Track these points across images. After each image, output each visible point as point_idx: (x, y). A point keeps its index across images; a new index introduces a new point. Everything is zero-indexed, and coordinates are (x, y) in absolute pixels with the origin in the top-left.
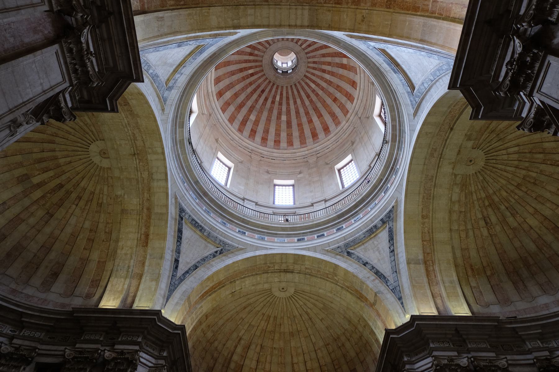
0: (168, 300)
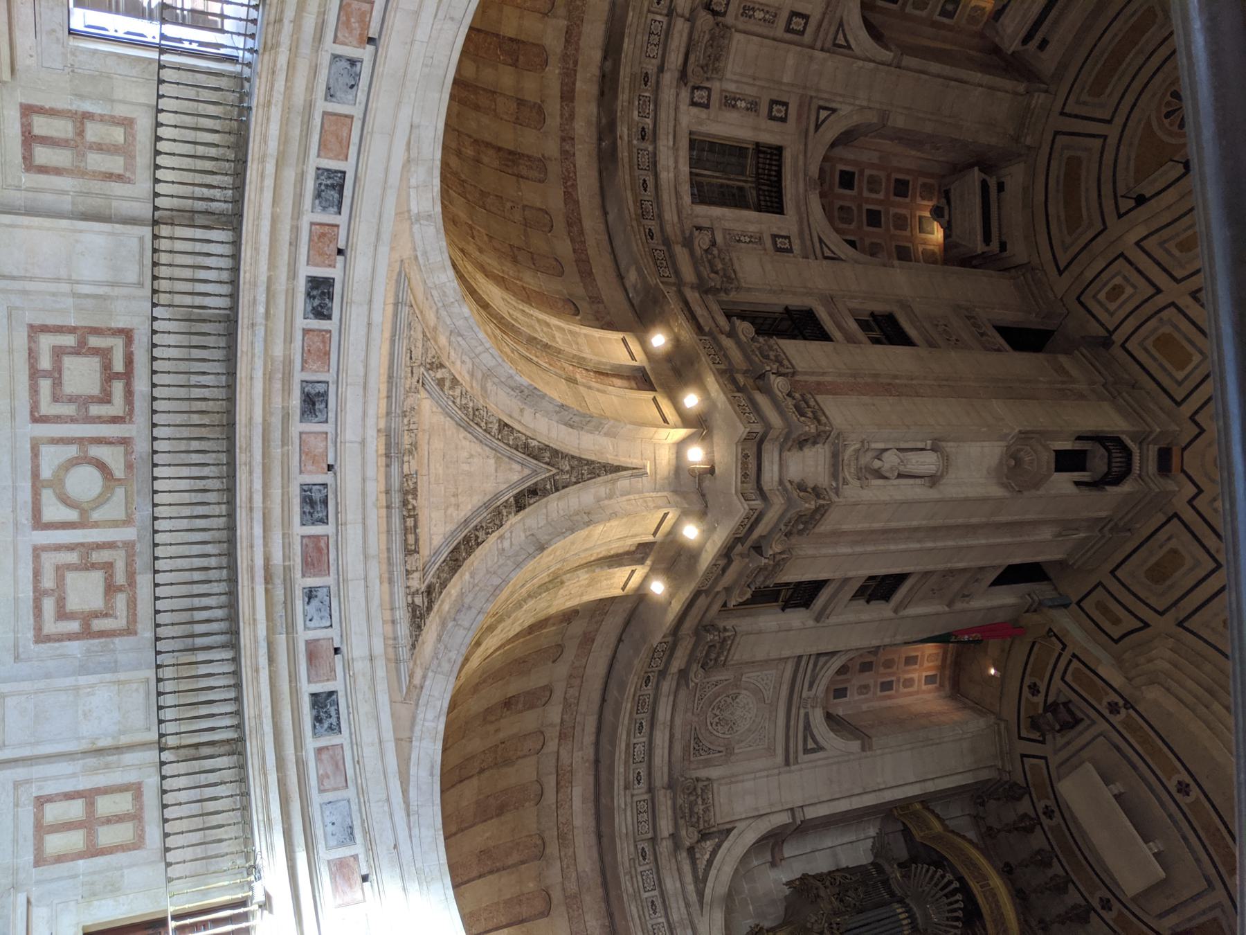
0: (618, 469)
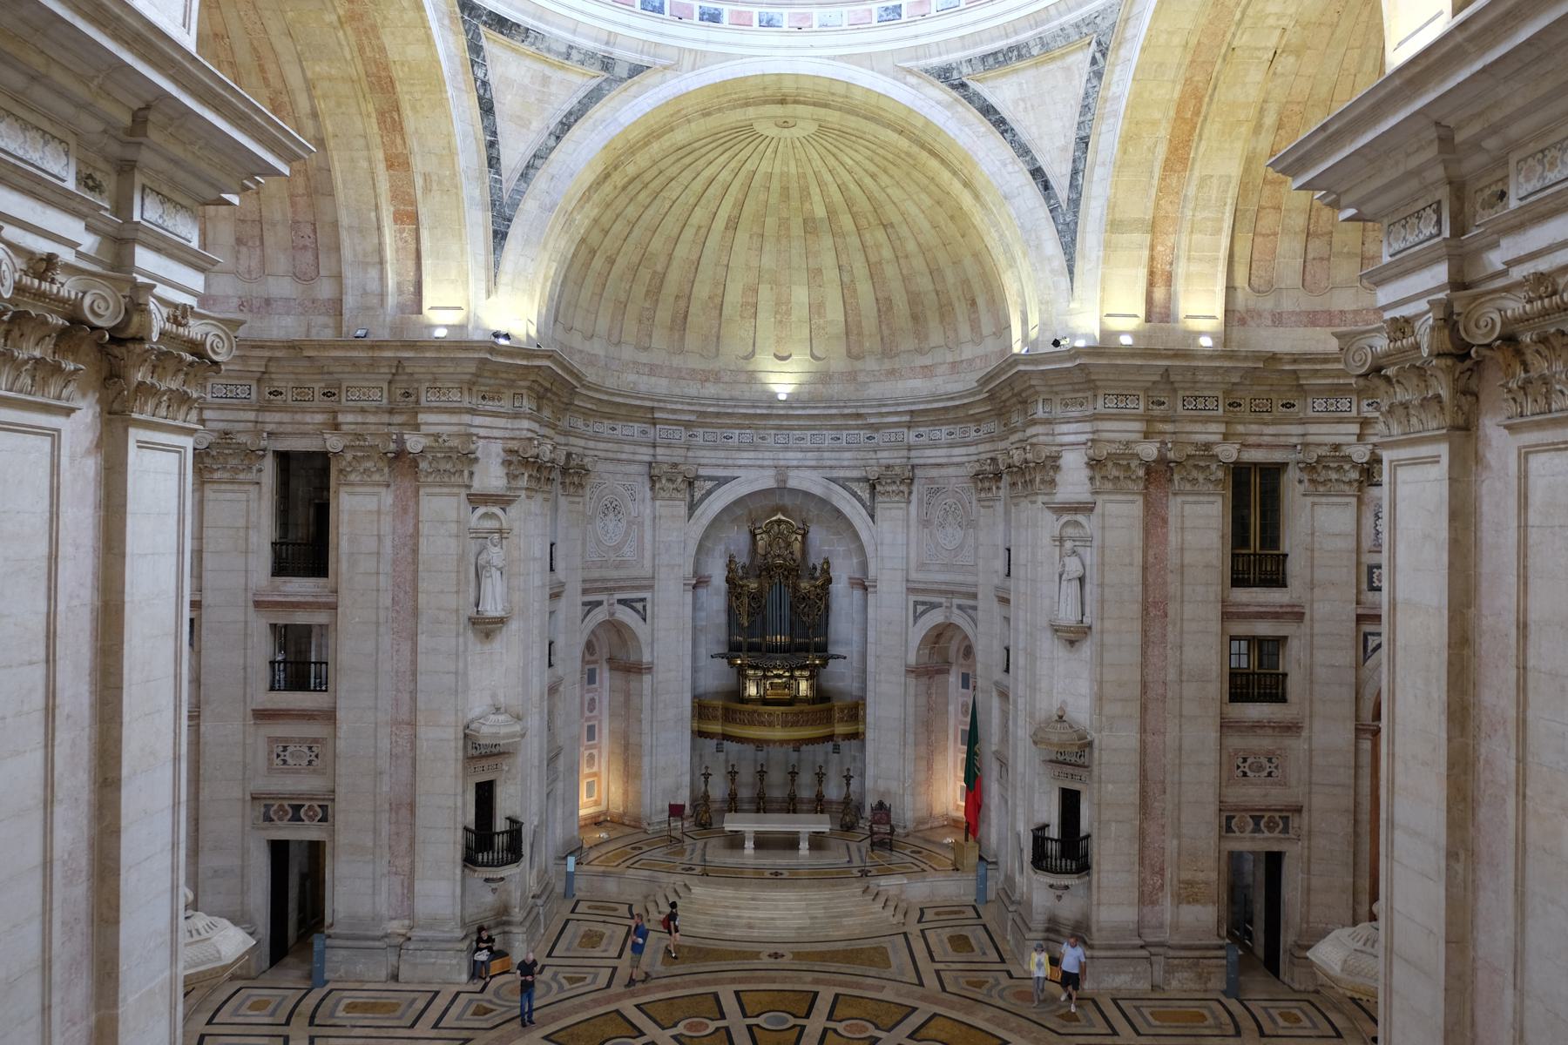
0: (1071, 272)
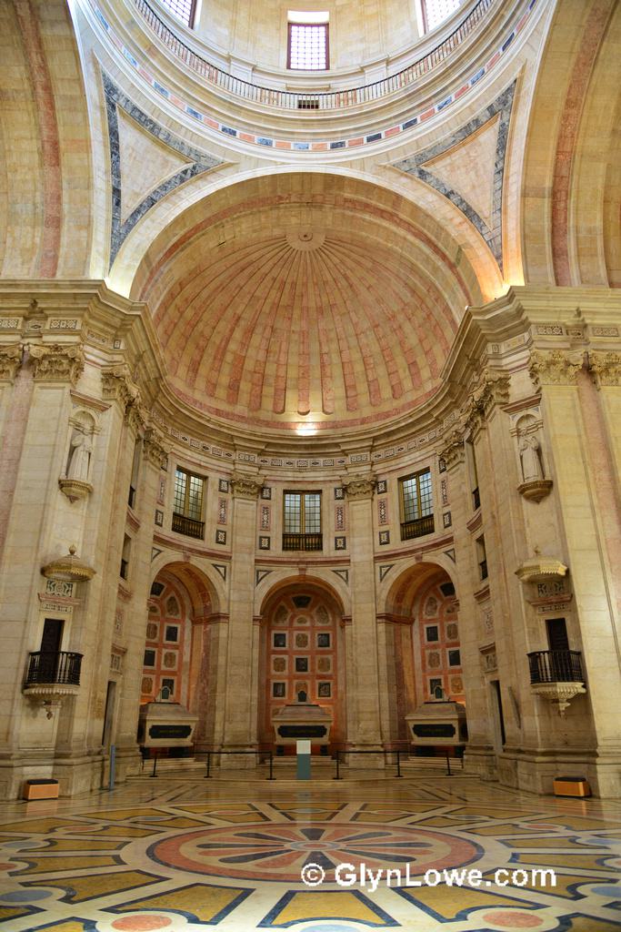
0: (112, 260)
